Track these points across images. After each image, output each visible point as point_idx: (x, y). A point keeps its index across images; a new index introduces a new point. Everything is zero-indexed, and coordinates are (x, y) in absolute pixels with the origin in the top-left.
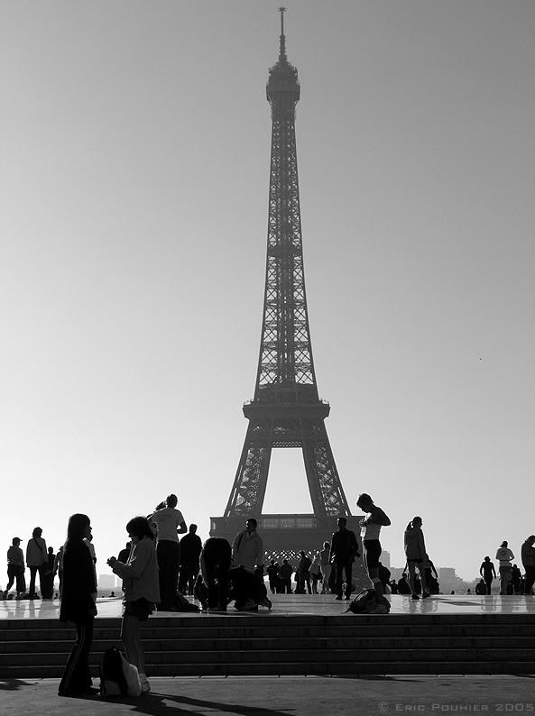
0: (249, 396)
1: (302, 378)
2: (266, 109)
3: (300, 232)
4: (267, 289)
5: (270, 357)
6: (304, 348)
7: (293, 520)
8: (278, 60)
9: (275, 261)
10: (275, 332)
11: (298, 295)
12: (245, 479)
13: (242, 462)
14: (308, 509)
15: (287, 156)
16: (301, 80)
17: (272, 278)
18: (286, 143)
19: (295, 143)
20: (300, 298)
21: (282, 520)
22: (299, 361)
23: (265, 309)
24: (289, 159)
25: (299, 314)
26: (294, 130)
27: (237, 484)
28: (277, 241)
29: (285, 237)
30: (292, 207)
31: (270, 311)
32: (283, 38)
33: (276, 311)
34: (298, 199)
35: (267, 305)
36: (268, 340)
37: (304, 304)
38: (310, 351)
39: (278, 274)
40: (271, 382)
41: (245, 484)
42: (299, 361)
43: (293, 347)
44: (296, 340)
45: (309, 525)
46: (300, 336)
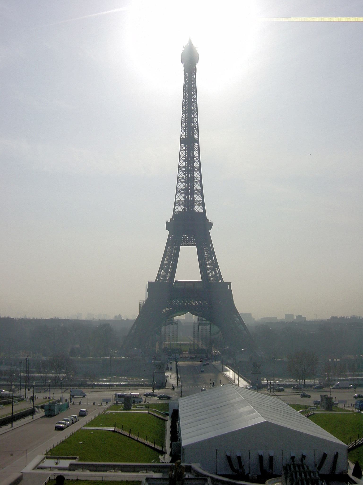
0: (169, 217)
1: (198, 209)
3: (198, 131)
5: (181, 197)
6: (200, 192)
9: (185, 146)
10: (184, 184)
11: (196, 164)
25: (197, 175)
28: (185, 136)
30: (193, 118)
31: (181, 173)
35: (180, 168)
36: (179, 188)
39: (185, 153)
43: (192, 194)
46: (197, 186)
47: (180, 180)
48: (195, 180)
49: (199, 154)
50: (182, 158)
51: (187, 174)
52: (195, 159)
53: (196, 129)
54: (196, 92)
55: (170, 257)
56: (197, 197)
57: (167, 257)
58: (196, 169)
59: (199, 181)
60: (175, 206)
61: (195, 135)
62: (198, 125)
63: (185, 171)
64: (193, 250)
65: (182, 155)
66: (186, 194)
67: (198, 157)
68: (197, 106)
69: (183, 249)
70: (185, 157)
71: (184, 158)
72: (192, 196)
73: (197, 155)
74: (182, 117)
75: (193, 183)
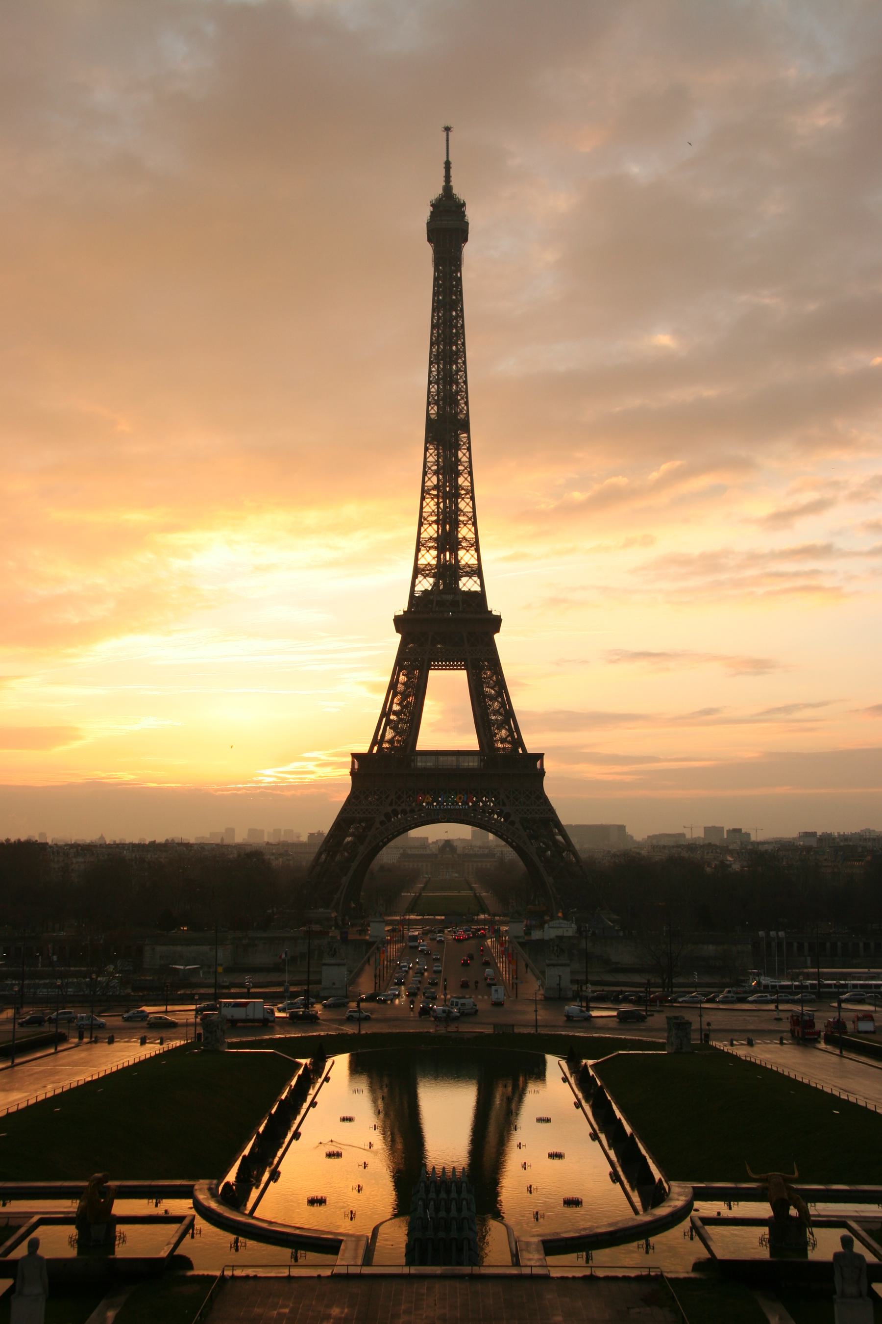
1: (468, 584)
2: (427, 251)
3: (467, 403)
4: (425, 474)
5: (429, 558)
6: (472, 545)
7: (454, 758)
8: (440, 191)
10: (435, 526)
12: (396, 708)
13: (393, 685)
14: (476, 747)
16: (471, 214)
18: (451, 293)
21: (441, 758)
22: (463, 563)
23: (423, 499)
24: (454, 313)
26: (460, 279)
27: (385, 714)
29: (448, 409)
30: (457, 374)
31: (428, 501)
32: (448, 165)
33: (436, 500)
35: (424, 492)
36: (425, 535)
38: (477, 550)
39: (438, 455)
40: (430, 589)
41: (395, 713)
44: (460, 536)
45: (473, 763)
46: (465, 532)
47: (425, 519)
48: (461, 518)
50: (430, 468)
52: (460, 468)
54: (462, 310)
55: (405, 696)
56: (466, 557)
57: (399, 697)
58: (463, 492)
59: (470, 519)
60: (415, 577)
61: (461, 411)
63: (437, 496)
65: (431, 459)
66: (441, 550)
67: (466, 465)
68: (464, 344)
69: (434, 675)
70: (438, 465)
71: (435, 468)
72: (454, 551)
73: (465, 459)
74: (430, 372)
75: (455, 524)
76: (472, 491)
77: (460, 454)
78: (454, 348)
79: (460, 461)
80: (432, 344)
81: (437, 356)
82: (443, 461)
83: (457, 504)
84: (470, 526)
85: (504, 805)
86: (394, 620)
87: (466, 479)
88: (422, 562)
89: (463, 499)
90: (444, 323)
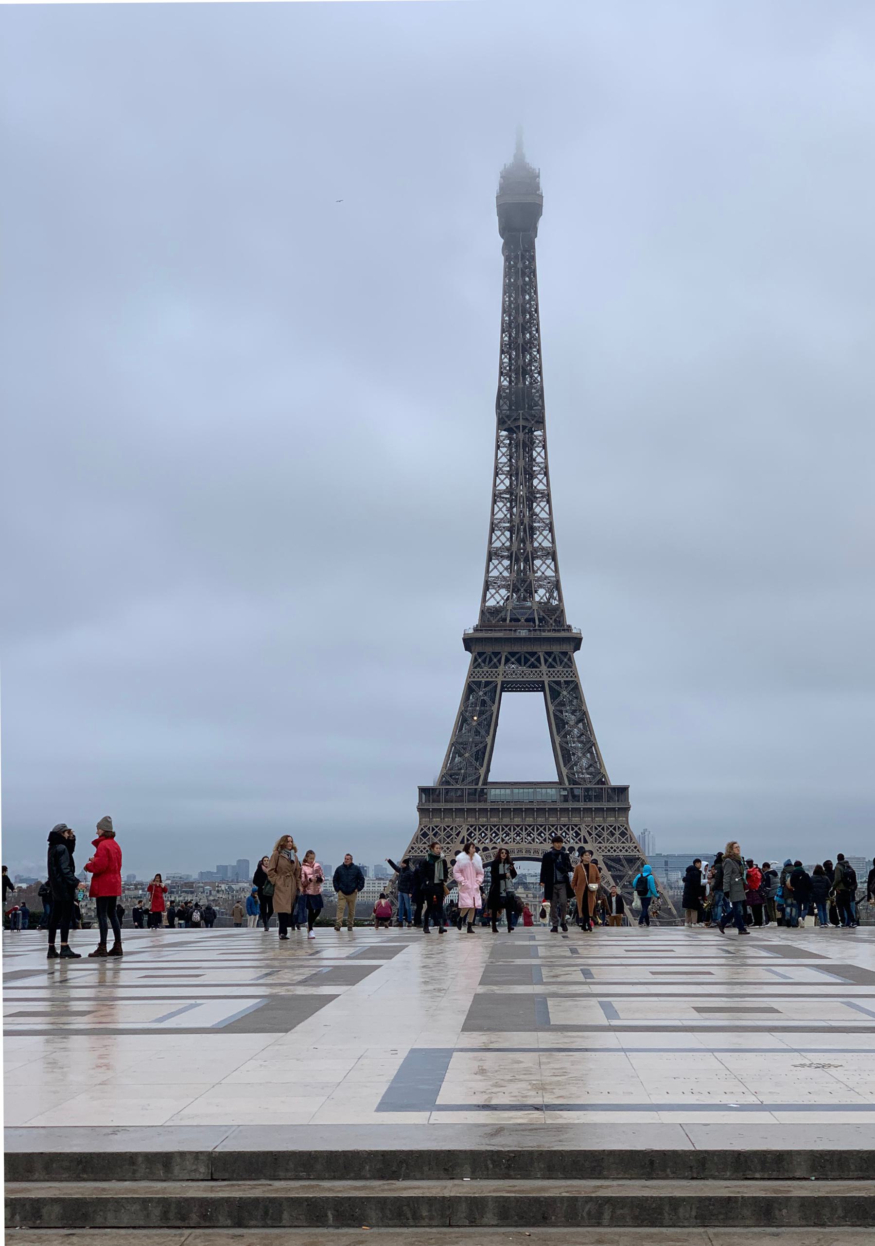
0: (471, 620)
4: (496, 474)
5: (501, 568)
10: (508, 534)
11: (538, 484)
15: (524, 292)
17: (504, 460)
19: (535, 276)
20: (541, 487)
21: (516, 791)
22: (539, 574)
23: (494, 502)
24: (527, 297)
30: (530, 364)
31: (501, 504)
33: (508, 505)
34: (539, 351)
35: (496, 497)
36: (497, 544)
37: (547, 497)
38: (554, 559)
40: (501, 603)
42: (539, 574)
43: (529, 558)
44: (536, 544)
46: (542, 540)
47: (496, 525)
49: (546, 458)
50: (501, 469)
51: (515, 510)
52: (534, 469)
53: (537, 391)
54: (536, 292)
56: (542, 568)
58: (538, 496)
59: (547, 525)
60: (487, 588)
62: (541, 378)
64: (537, 699)
66: (514, 558)
67: (542, 466)
70: (511, 466)
71: (508, 469)
74: (501, 363)
76: (549, 495)
77: (535, 454)
78: (528, 336)
79: (535, 460)
80: (503, 331)
81: (510, 344)
82: (517, 461)
83: (531, 509)
84: (545, 533)
85: (586, 842)
86: (464, 640)
87: (541, 481)
88: (494, 573)
89: (538, 505)
90: (516, 309)
